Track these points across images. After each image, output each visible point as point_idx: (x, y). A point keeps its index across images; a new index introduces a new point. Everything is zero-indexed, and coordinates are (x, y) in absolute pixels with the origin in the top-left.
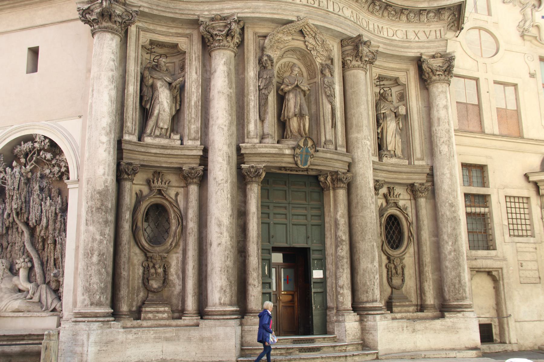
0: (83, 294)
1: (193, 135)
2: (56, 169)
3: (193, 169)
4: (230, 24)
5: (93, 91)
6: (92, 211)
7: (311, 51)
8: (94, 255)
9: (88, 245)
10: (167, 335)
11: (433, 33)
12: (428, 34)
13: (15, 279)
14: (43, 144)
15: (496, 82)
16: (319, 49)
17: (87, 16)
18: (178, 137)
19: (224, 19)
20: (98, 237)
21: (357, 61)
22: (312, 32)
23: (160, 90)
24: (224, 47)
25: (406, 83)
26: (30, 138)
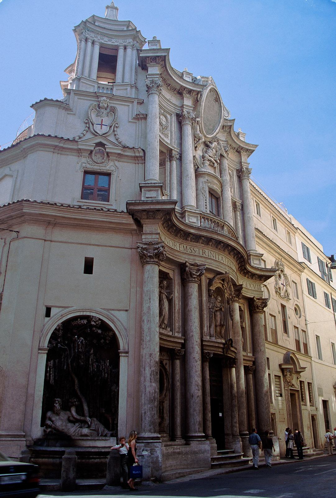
0: (150, 426)
1: (177, 331)
2: (102, 341)
3: (179, 350)
4: (201, 270)
5: (150, 299)
6: (154, 374)
7: (224, 290)
8: (156, 401)
9: (152, 395)
10: (178, 450)
11: (257, 286)
12: (255, 286)
13: (68, 412)
14: (97, 323)
15: (270, 314)
16: (228, 290)
17: (144, 251)
18: (169, 329)
19: (198, 266)
20: (157, 390)
21: (237, 298)
22: (228, 281)
23: (164, 301)
24: (195, 282)
25: (243, 310)
26: (88, 318)
